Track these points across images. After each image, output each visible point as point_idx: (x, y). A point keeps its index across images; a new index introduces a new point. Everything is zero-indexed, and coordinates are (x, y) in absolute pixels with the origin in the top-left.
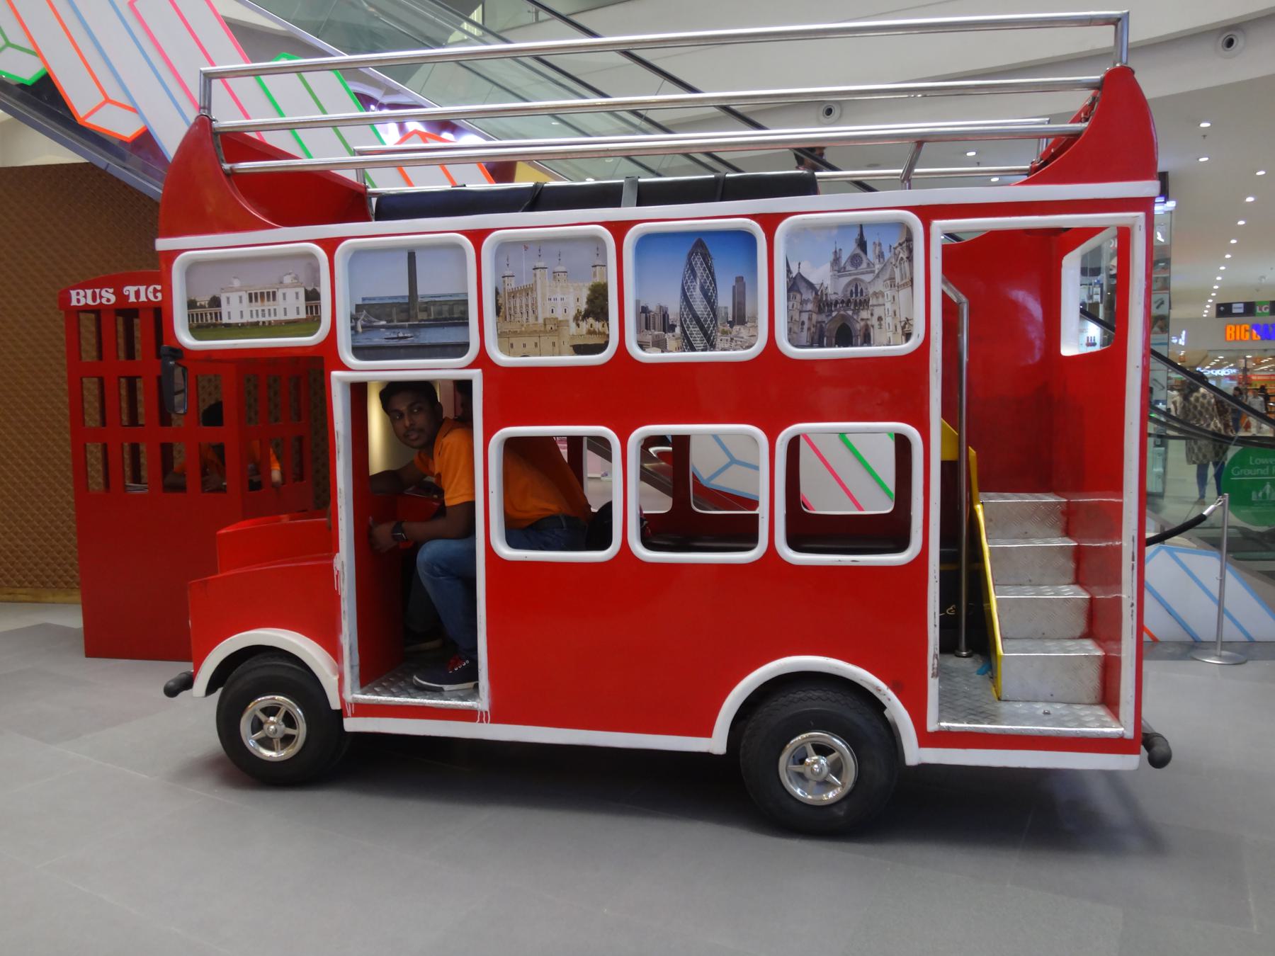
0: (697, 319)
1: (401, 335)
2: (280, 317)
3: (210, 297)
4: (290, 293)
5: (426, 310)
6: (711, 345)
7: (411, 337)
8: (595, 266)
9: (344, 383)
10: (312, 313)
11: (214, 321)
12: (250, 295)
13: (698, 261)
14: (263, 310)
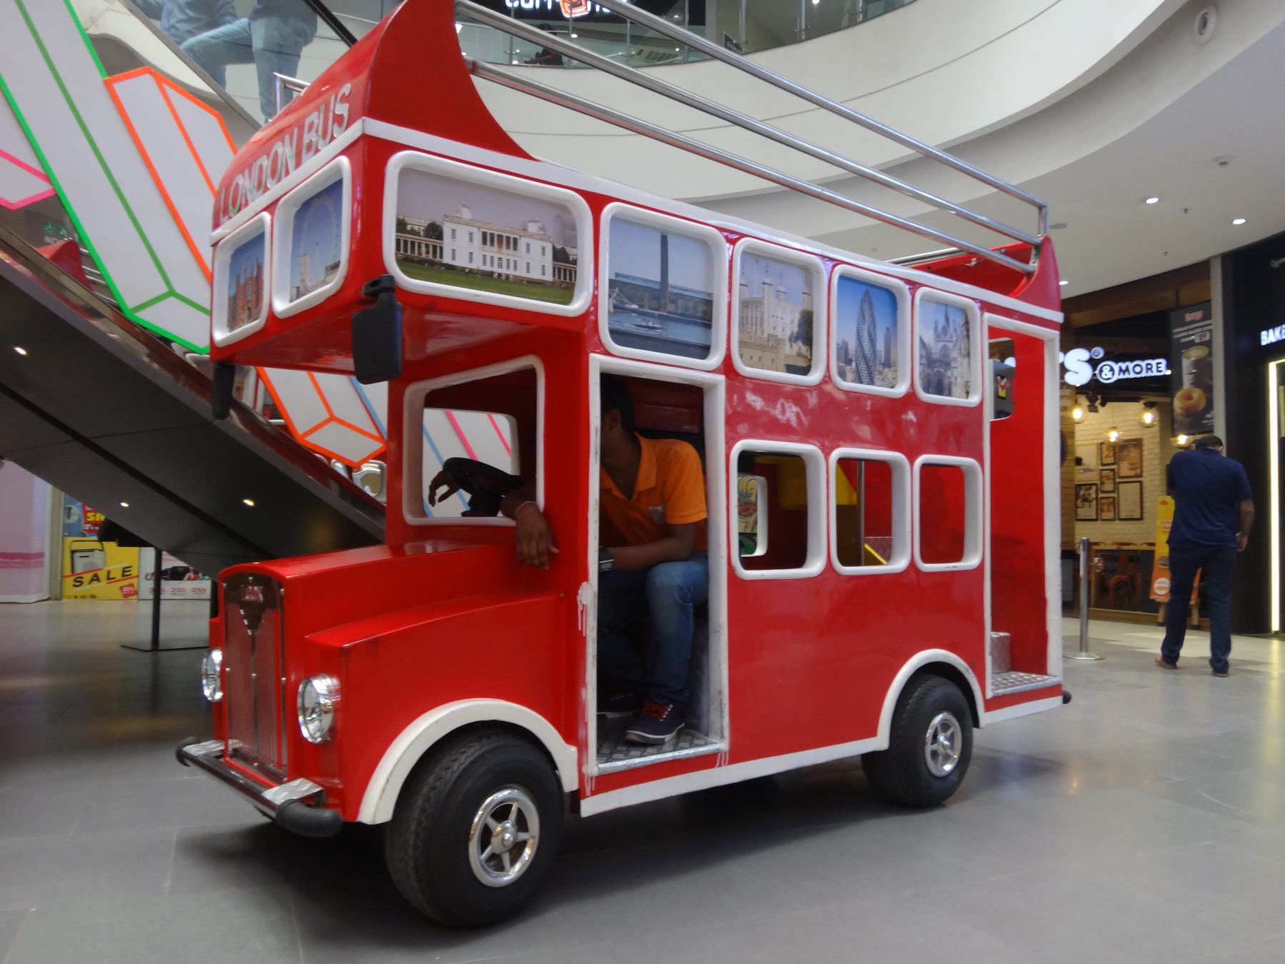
0: (865, 357)
1: (650, 324)
2: (522, 272)
3: (428, 222)
4: (536, 245)
5: (674, 302)
6: (871, 382)
7: (660, 329)
10: (559, 278)
11: (431, 256)
12: (484, 235)
13: (866, 307)
14: (500, 259)
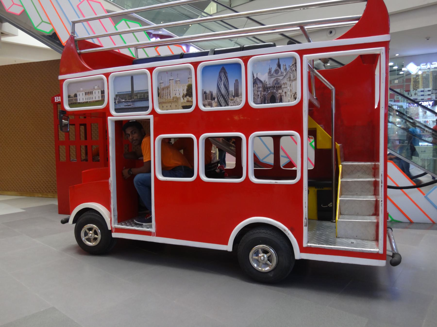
0: (222, 95)
1: (129, 104)
2: (94, 100)
3: (74, 94)
4: (97, 91)
5: (136, 95)
6: (227, 105)
7: (132, 105)
8: (189, 78)
9: (112, 121)
10: (103, 98)
12: (85, 93)
13: (222, 74)
14: (89, 98)
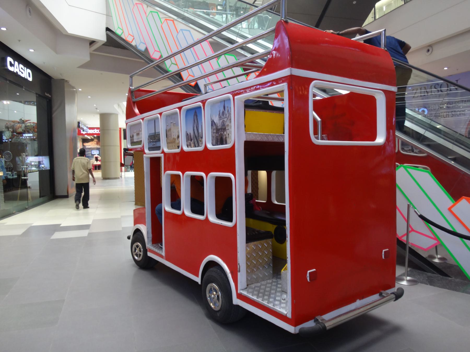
0: (196, 136)
9: (147, 158)
13: (195, 117)
